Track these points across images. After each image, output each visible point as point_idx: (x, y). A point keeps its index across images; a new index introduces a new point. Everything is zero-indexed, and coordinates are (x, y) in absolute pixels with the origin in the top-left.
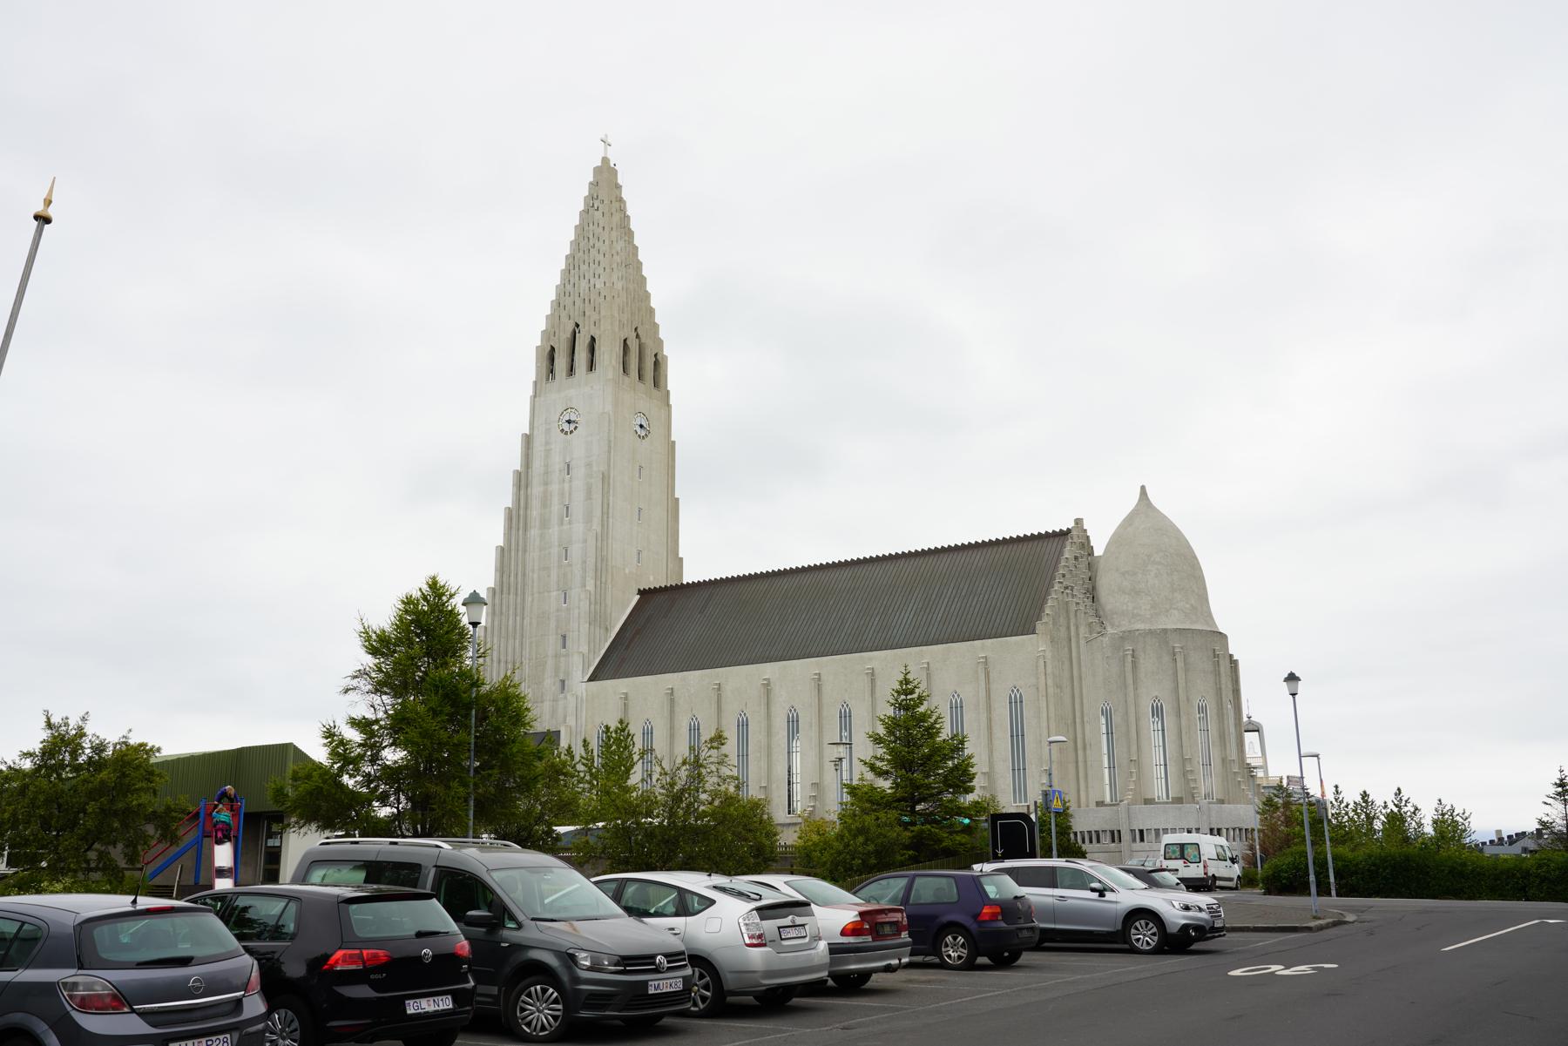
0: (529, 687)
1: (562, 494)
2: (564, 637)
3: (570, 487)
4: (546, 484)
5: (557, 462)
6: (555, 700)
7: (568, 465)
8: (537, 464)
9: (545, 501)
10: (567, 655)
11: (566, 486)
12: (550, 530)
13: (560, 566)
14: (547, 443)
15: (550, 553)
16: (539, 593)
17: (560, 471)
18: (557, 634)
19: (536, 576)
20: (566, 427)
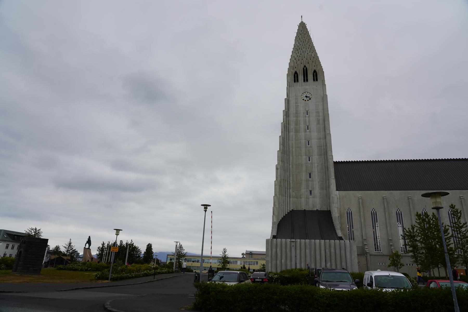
0: (293, 192)
1: (305, 122)
2: (310, 174)
3: (309, 120)
4: (297, 117)
5: (302, 109)
6: (307, 198)
7: (307, 112)
8: (292, 110)
9: (297, 123)
10: (312, 181)
11: (307, 119)
12: (300, 134)
13: (306, 147)
14: (296, 103)
15: (301, 142)
16: (296, 156)
17: (304, 113)
18: (306, 172)
19: (294, 150)
20: (305, 99)
